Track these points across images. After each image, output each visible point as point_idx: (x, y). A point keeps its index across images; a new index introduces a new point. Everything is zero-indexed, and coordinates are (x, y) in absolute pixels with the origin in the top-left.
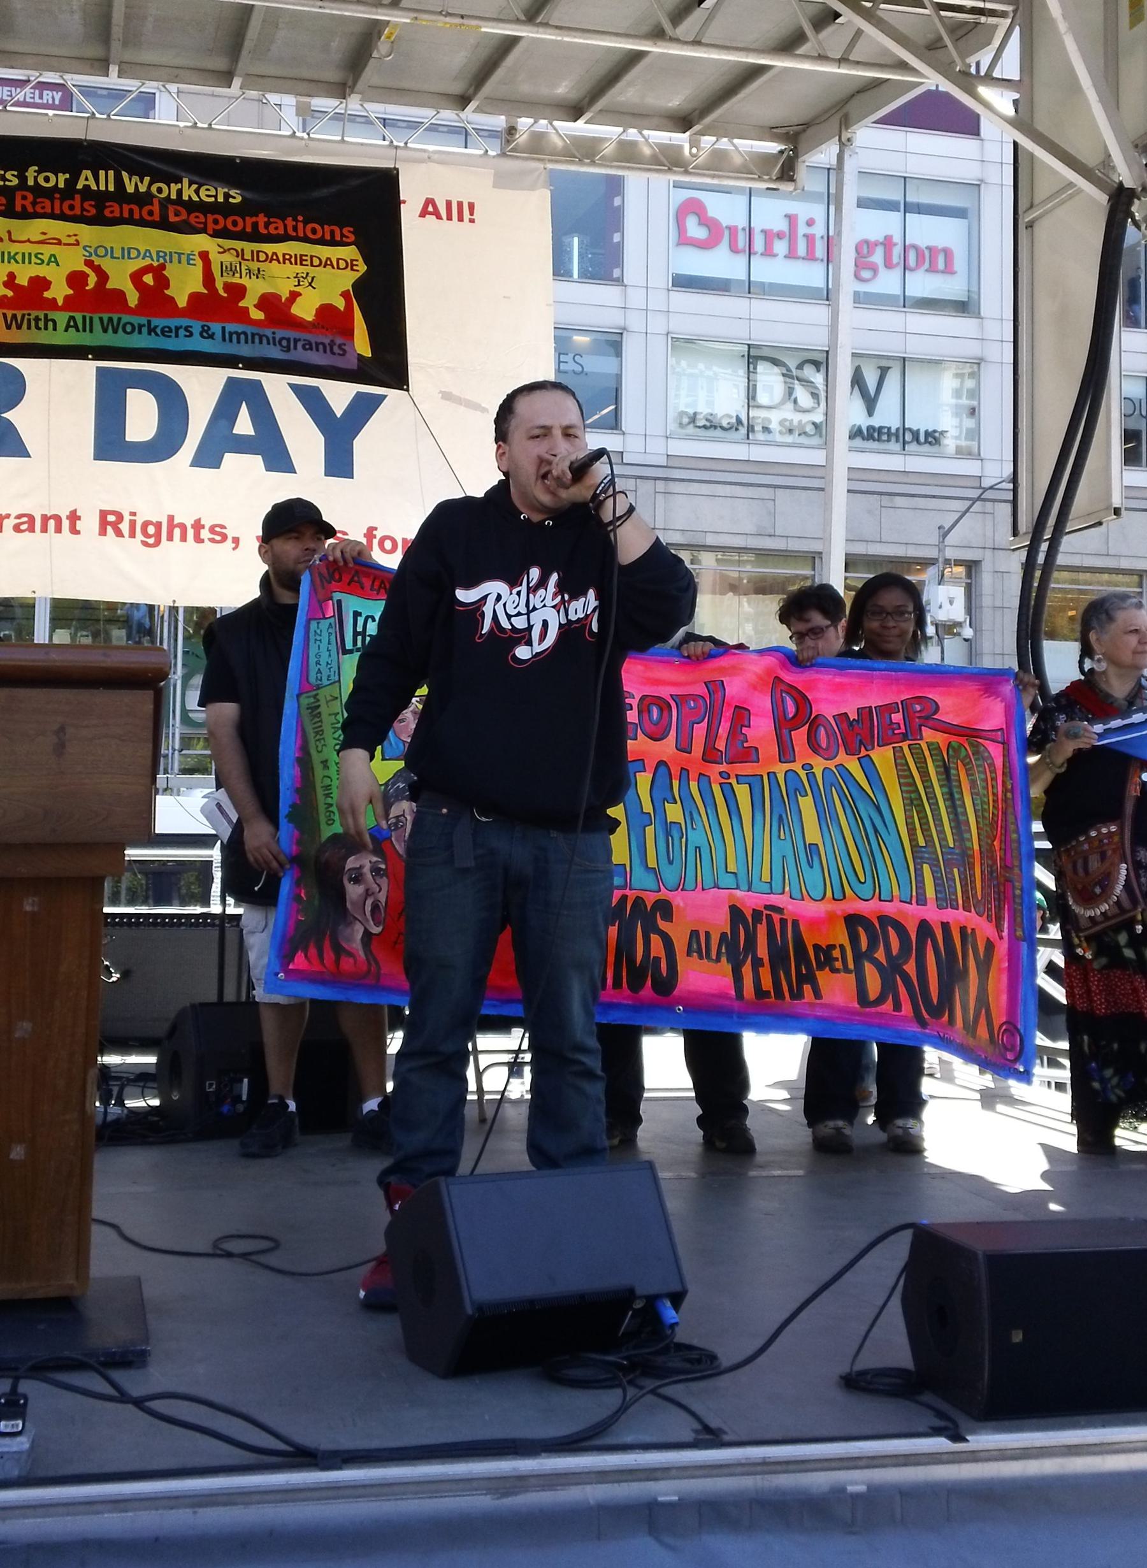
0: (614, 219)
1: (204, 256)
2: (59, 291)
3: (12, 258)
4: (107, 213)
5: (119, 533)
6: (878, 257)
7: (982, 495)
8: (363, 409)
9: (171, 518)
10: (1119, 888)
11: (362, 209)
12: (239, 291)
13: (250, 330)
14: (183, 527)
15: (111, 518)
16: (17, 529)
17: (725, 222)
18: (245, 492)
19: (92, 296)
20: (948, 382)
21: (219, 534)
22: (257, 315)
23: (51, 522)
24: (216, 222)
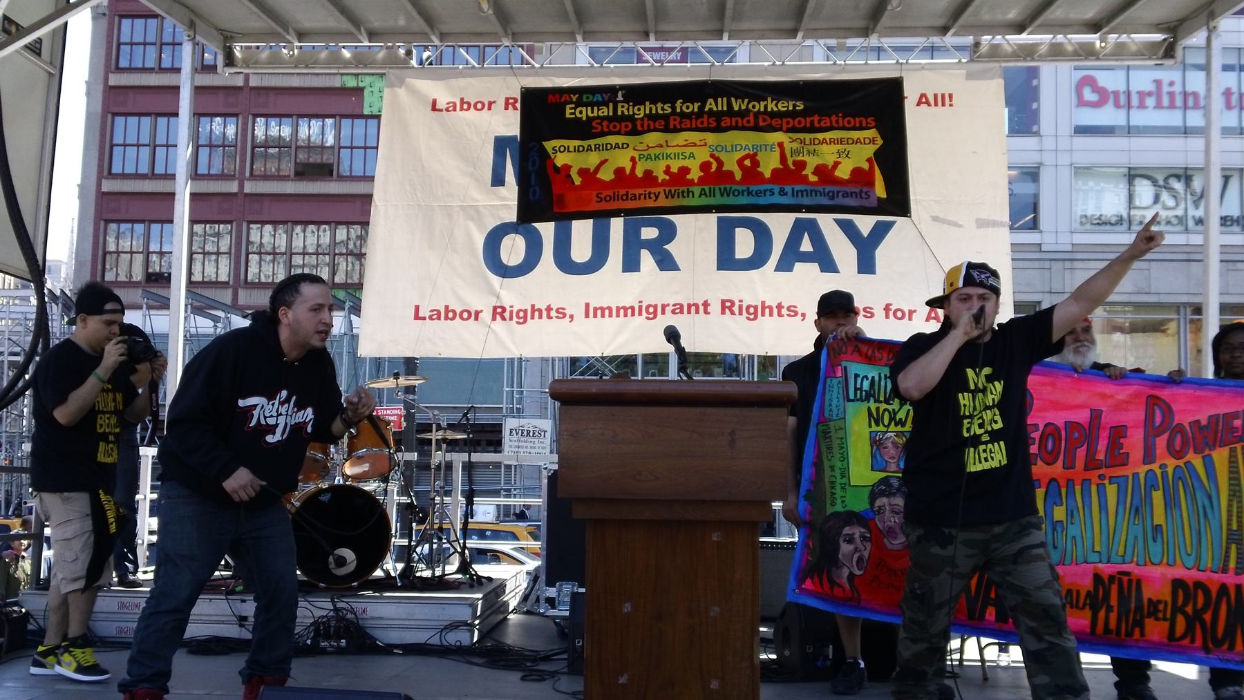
0: (1034, 94)
1: (781, 145)
3: (668, 156)
4: (723, 124)
8: (880, 231)
9: (763, 303)
12: (801, 165)
13: (809, 188)
14: (771, 308)
15: (728, 304)
17: (1110, 88)
18: (808, 284)
19: (715, 176)
21: (793, 312)
22: (813, 178)
24: (788, 123)
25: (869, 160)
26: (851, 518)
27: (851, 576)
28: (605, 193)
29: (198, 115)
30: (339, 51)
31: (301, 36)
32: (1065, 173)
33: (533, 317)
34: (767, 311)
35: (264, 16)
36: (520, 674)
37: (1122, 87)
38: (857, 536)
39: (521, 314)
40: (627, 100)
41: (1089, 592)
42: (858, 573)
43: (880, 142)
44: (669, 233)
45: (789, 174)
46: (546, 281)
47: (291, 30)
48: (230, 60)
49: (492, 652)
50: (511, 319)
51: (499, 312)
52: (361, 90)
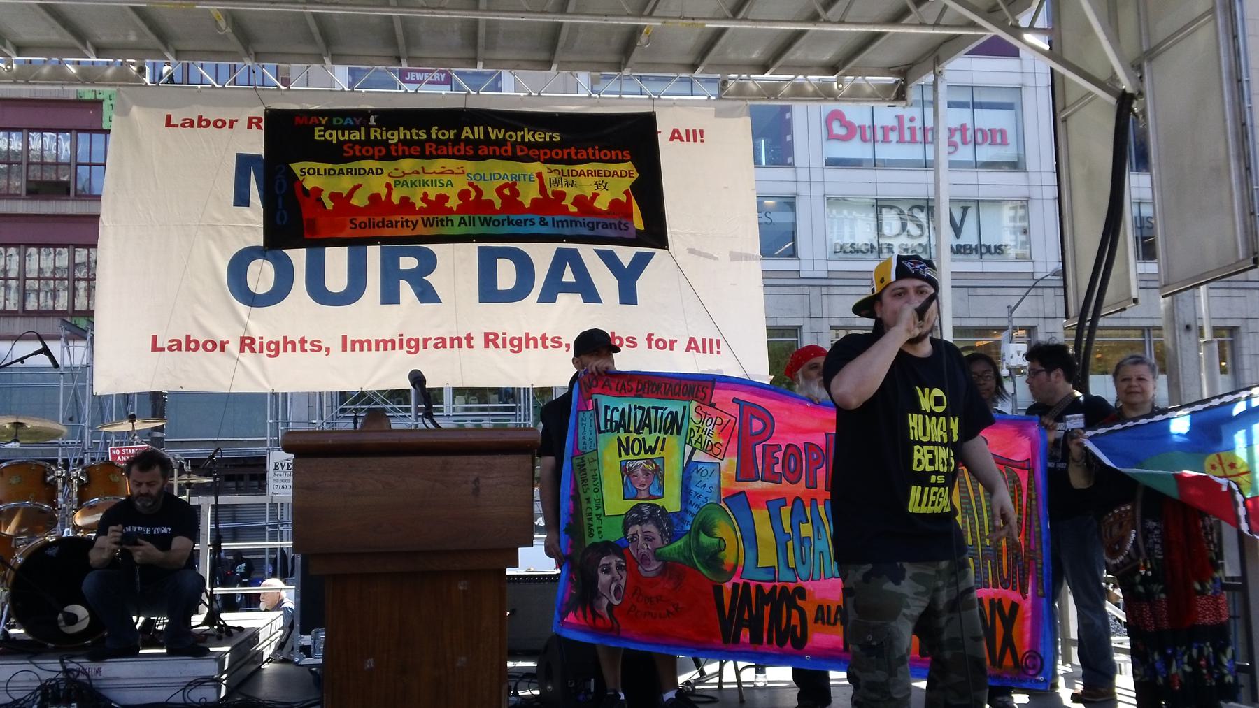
0: (787, 127)
1: (539, 175)
2: (454, 202)
3: (425, 183)
5: (496, 346)
6: (957, 138)
7: (1035, 284)
8: (641, 263)
9: (527, 335)
10: (1129, 546)
11: (634, 139)
12: (562, 195)
13: (569, 218)
14: (535, 339)
15: (491, 337)
16: (436, 346)
18: (570, 317)
19: (473, 205)
20: (1007, 213)
22: (573, 209)
23: (456, 342)
24: (545, 154)
25: (626, 192)
26: (607, 548)
27: (610, 605)
28: (360, 219)
32: (819, 203)
33: (285, 350)
34: (289, 346)
37: (867, 123)
38: (613, 566)
40: (379, 125)
41: (839, 607)
42: (617, 603)
43: (636, 175)
44: (429, 263)
45: (549, 204)
46: (298, 313)
50: (261, 351)
51: (247, 343)
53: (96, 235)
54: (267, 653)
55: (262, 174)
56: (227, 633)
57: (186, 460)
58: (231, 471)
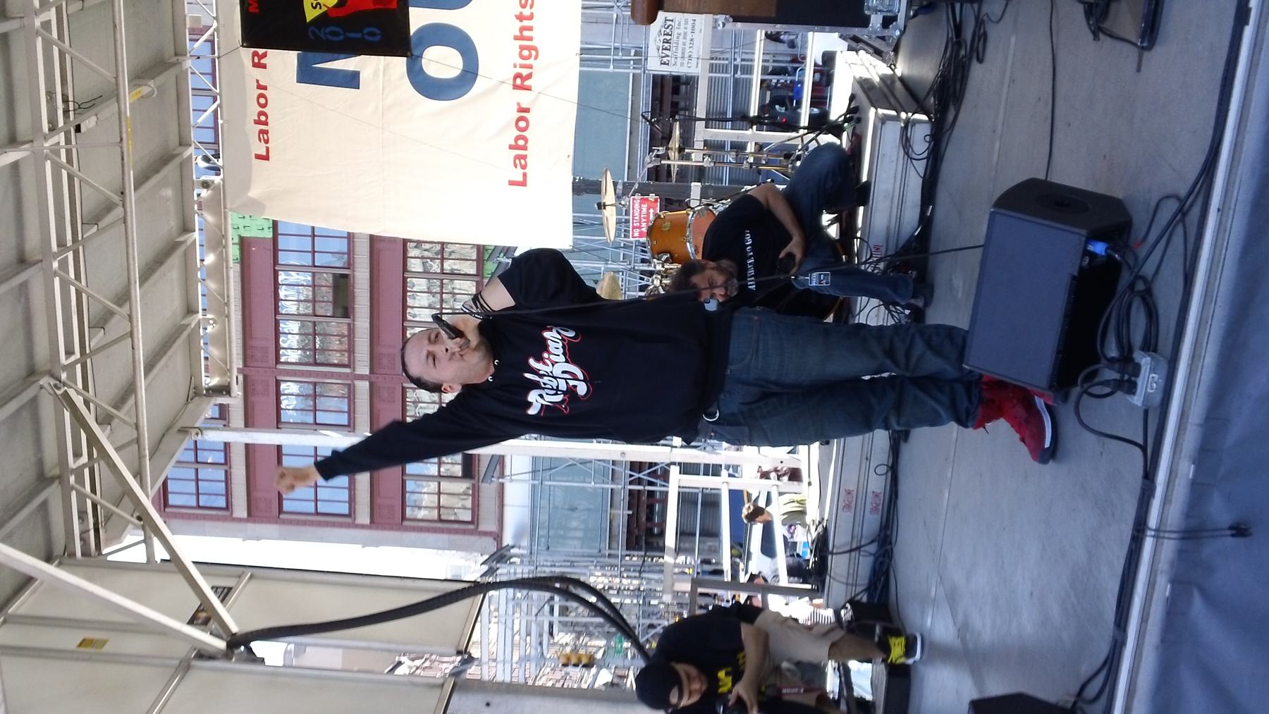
29: (278, 424)
30: (208, 268)
31: (190, 310)
33: (530, 39)
35: (170, 353)
36: (975, 63)
39: (526, 53)
47: (185, 322)
48: (224, 390)
49: (943, 98)
50: (530, 67)
51: (521, 82)
52: (242, 239)
53: (393, 240)
54: (883, 69)
55: (319, 55)
56: (854, 114)
57: (651, 151)
58: (667, 108)
